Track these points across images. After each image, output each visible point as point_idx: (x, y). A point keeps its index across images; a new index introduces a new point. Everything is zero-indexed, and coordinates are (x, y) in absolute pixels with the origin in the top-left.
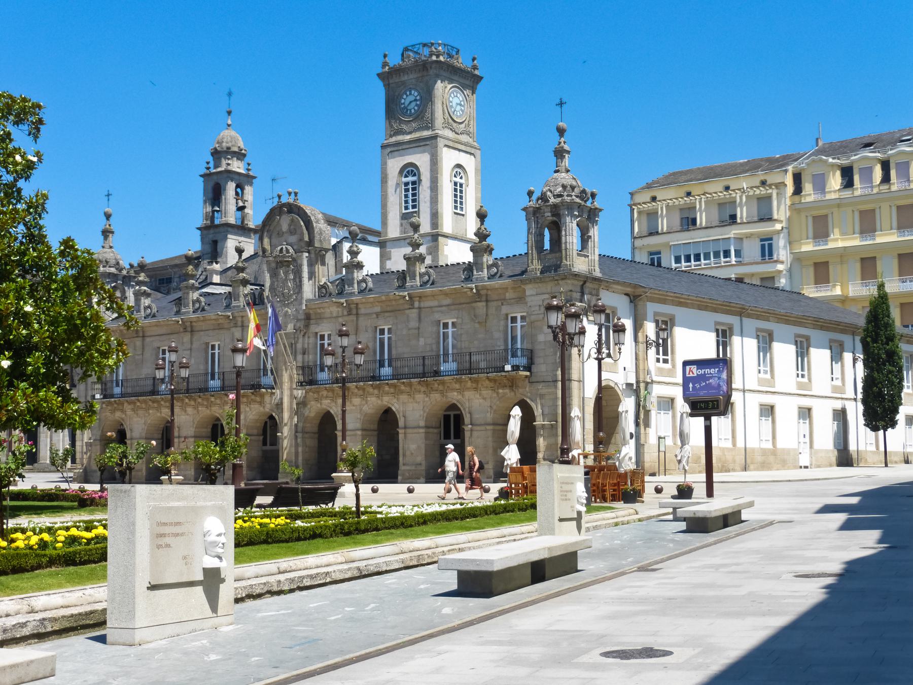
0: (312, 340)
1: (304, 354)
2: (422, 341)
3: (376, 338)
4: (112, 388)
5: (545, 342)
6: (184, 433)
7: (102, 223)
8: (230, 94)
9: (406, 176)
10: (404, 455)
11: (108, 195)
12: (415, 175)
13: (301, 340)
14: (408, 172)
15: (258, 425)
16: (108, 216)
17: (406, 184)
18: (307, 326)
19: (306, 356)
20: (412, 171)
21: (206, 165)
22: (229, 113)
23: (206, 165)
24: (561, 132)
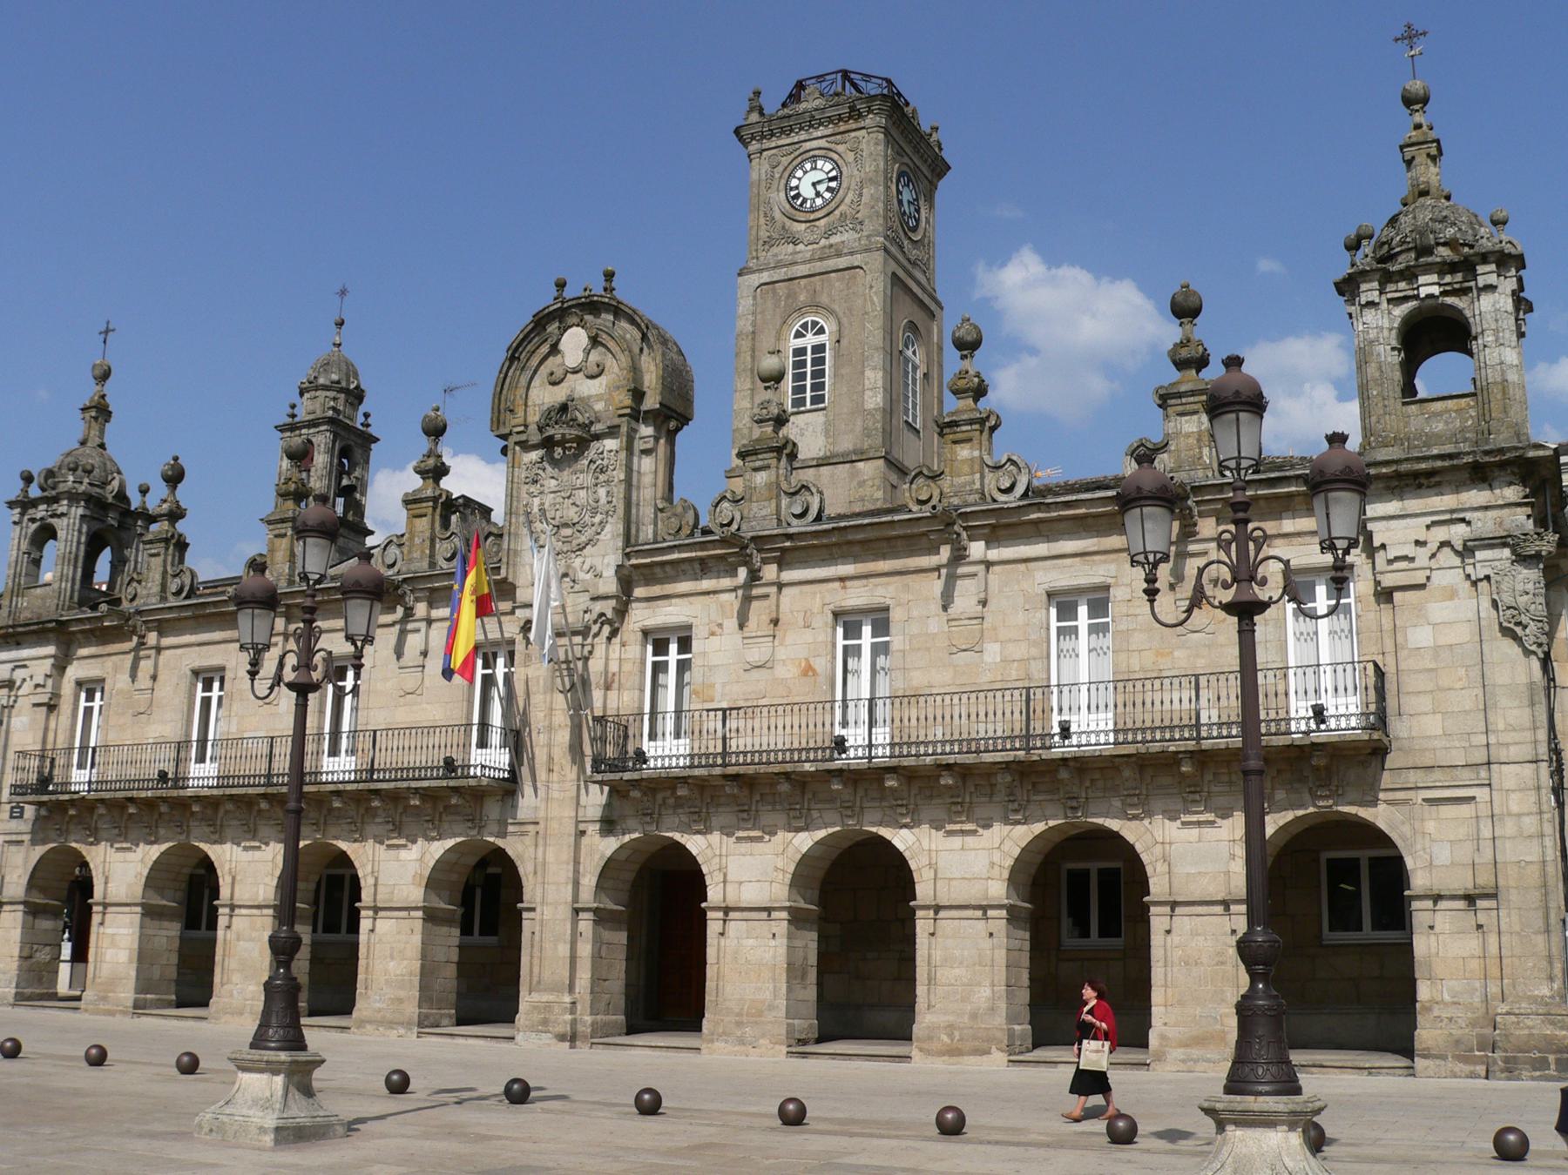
0: (633, 650)
1: (608, 688)
2: (992, 652)
3: (834, 645)
4: (69, 766)
5: (1437, 649)
6: (242, 895)
7: (88, 391)
8: (343, 293)
9: (799, 335)
10: (931, 980)
11: (107, 332)
12: (821, 331)
13: (600, 650)
14: (805, 326)
15: (454, 877)
16: (104, 376)
17: (800, 352)
18: (622, 612)
19: (612, 695)
20: (815, 323)
21: (290, 411)
22: (340, 324)
23: (290, 411)
24: (1413, 101)
